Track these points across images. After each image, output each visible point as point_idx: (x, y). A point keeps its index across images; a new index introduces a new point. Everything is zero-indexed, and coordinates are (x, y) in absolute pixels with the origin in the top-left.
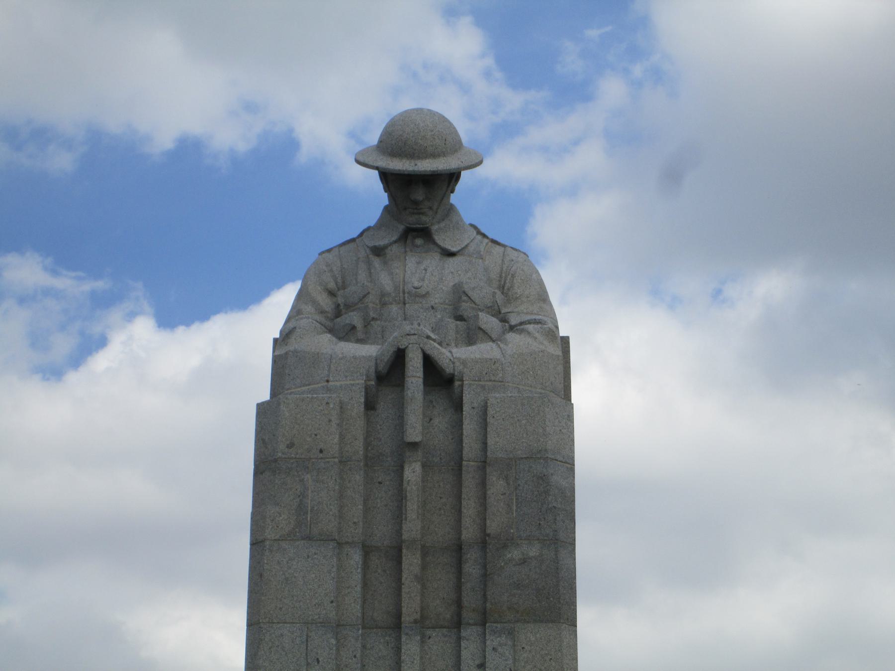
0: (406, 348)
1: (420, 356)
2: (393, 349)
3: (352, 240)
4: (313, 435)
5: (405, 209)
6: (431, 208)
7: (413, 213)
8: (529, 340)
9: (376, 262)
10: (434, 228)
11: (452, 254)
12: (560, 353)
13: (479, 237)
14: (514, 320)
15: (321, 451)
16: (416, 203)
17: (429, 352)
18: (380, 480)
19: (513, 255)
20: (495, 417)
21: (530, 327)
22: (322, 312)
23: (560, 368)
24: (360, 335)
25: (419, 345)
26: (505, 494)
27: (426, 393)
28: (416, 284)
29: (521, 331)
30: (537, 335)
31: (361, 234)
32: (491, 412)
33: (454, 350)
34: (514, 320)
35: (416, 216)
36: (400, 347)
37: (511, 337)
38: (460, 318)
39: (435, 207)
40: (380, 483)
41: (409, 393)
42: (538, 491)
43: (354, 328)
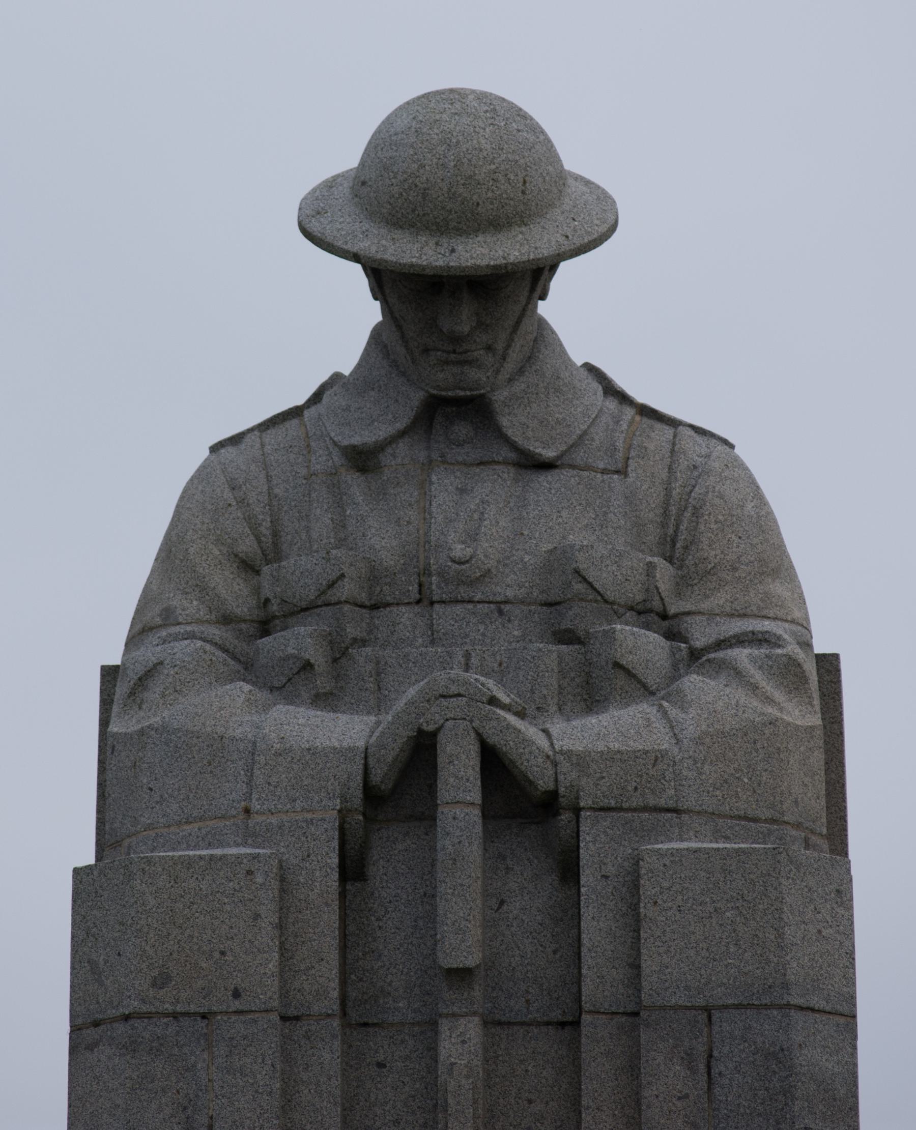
0: (438, 730)
1: (474, 749)
2: (406, 733)
3: (295, 413)
4: (217, 955)
5: (426, 351)
6: (489, 348)
7: (447, 363)
8: (740, 695)
9: (355, 484)
10: (499, 397)
11: (547, 466)
12: (816, 720)
13: (612, 404)
14: (700, 636)
15: (236, 994)
16: (456, 339)
17: (493, 740)
18: (381, 1058)
19: (694, 447)
20: (660, 902)
21: (742, 655)
22: (226, 620)
23: (818, 758)
24: (323, 683)
25: (471, 721)
26: (687, 1096)
27: (489, 837)
28: (459, 551)
29: (721, 666)
30: (758, 677)
31: (316, 397)
32: (648, 889)
33: (557, 727)
34: (700, 636)
35: (456, 370)
36: (425, 727)
37: (693, 682)
38: (567, 637)
39: (500, 346)
40: (381, 1065)
41: (446, 844)
42: (767, 1089)
43: (308, 666)
